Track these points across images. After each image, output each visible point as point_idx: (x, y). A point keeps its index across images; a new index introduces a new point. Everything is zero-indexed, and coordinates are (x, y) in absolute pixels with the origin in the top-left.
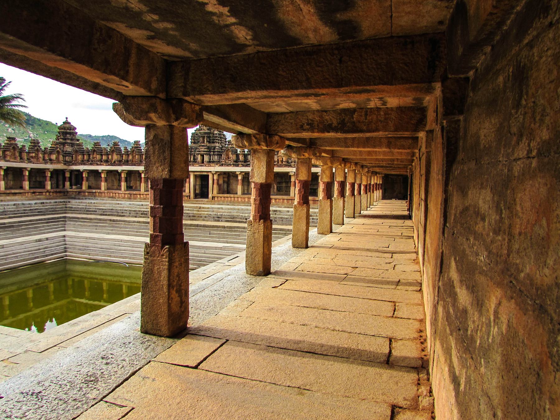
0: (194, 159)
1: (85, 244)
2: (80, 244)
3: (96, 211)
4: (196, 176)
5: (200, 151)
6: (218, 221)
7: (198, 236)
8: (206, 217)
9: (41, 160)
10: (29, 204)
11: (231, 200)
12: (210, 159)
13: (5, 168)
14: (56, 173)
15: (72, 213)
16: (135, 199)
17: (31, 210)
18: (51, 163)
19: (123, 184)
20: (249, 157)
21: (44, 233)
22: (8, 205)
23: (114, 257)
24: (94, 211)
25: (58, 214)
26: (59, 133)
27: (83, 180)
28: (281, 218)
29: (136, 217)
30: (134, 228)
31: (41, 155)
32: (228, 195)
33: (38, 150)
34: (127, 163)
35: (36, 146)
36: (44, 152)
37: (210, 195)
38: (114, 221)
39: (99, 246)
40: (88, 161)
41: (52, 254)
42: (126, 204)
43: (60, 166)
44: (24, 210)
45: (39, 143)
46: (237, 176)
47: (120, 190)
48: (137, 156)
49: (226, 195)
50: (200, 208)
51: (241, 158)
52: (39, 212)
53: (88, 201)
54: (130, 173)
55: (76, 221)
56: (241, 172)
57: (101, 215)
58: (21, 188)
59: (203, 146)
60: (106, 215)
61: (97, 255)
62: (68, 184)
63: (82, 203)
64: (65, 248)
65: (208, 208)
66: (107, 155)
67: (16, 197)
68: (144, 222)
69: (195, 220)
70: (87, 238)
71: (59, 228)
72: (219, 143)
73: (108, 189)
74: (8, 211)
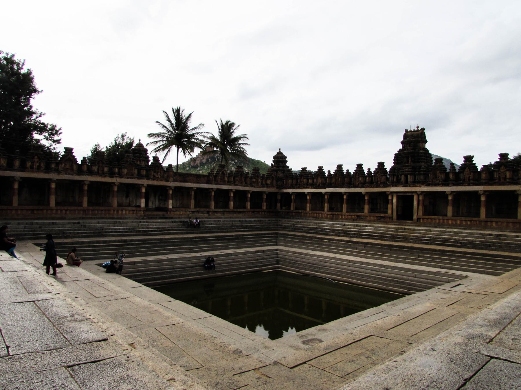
0: (397, 179)
1: (294, 258)
2: (290, 258)
3: (302, 229)
4: (398, 198)
5: (404, 172)
6: (427, 244)
7: (405, 258)
8: (411, 239)
9: (260, 184)
10: (250, 221)
11: (439, 222)
12: (415, 179)
13: (234, 191)
14: (270, 194)
15: (282, 230)
16: (337, 219)
17: (251, 226)
18: (267, 187)
19: (326, 205)
20: (462, 175)
21: (261, 246)
22: (235, 221)
23: (321, 272)
24: (301, 229)
25: (271, 230)
26: (273, 161)
27: (291, 202)
28: (508, 243)
29: (339, 236)
30: (337, 246)
31: (260, 181)
32: (436, 217)
33: (258, 176)
34: (330, 186)
35: (256, 173)
36: (263, 177)
37: (415, 217)
38: (319, 238)
39: (307, 261)
40: (296, 185)
41: (267, 265)
42: (329, 224)
43: (273, 190)
44: (246, 226)
45: (259, 170)
46: (447, 196)
47: (324, 211)
49: (433, 217)
50: (405, 229)
51: (451, 176)
52: (257, 228)
53: (295, 220)
55: (287, 238)
56: (452, 192)
57: (307, 233)
58: (245, 207)
59: (407, 166)
60: (311, 233)
61: (305, 269)
62: (279, 205)
63: (290, 221)
64: (278, 260)
65: (414, 230)
66: (313, 179)
67: (241, 215)
69: (400, 241)
70: (295, 253)
71: (272, 242)
72: (424, 162)
73: (312, 209)
74: (235, 226)
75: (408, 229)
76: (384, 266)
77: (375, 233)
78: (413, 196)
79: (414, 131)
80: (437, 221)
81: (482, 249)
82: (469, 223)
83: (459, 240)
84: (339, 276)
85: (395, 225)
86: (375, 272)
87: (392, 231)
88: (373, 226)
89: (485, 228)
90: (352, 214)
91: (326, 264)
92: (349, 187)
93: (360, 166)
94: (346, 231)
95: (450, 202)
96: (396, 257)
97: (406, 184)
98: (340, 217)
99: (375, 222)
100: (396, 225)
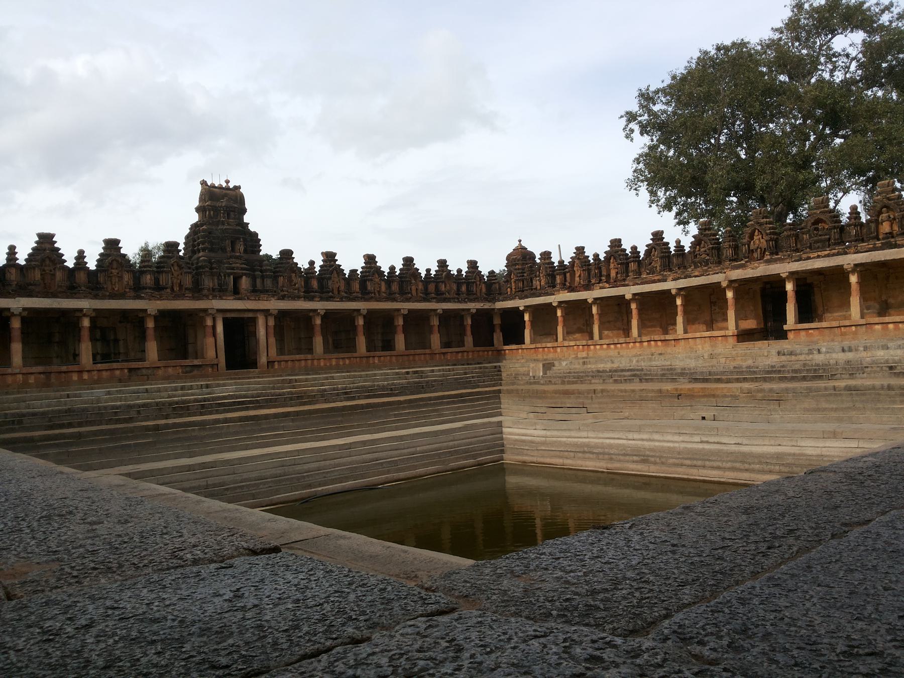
4: (226, 322)
5: (233, 269)
6: (353, 399)
12: (254, 285)
20: (330, 283)
29: (167, 417)
32: (302, 356)
34: (24, 290)
37: (263, 360)
48: (59, 275)
49: (298, 357)
54: (31, 318)
59: (237, 257)
61: (277, 492)
65: (306, 380)
68: (241, 419)
69: (310, 403)
70: (190, 468)
75: (296, 381)
76: (401, 438)
77: (245, 397)
78: (254, 321)
79: (220, 187)
80: (303, 363)
81: (421, 393)
82: (347, 362)
83: (383, 386)
84: (363, 477)
85: (231, 379)
86: (405, 451)
87: (274, 388)
88: (224, 385)
89: (368, 367)
90: (115, 365)
91: (306, 467)
92: (96, 297)
93: (112, 245)
94: (170, 404)
95: (318, 330)
96: (370, 425)
97: (236, 292)
98: (75, 377)
99: (178, 378)
100: (235, 379)
